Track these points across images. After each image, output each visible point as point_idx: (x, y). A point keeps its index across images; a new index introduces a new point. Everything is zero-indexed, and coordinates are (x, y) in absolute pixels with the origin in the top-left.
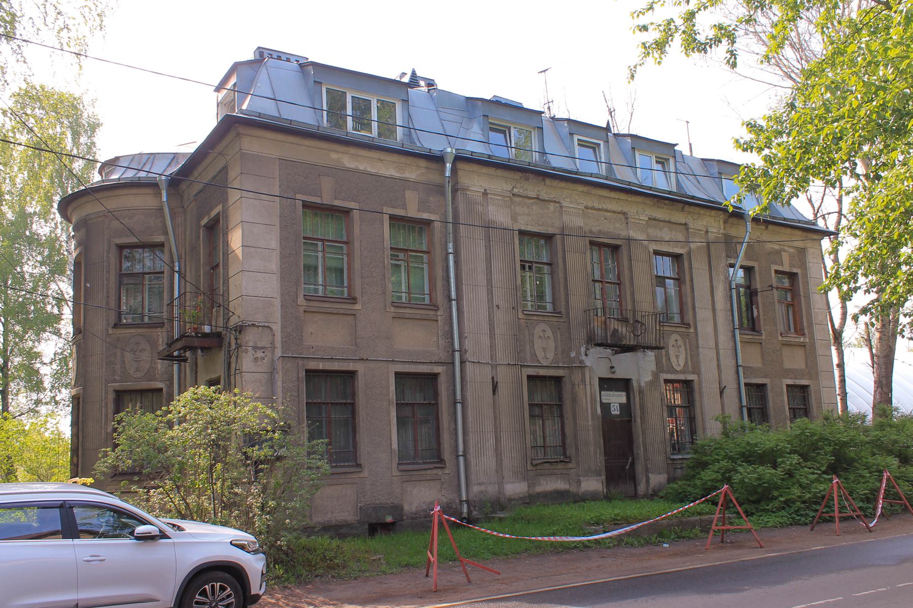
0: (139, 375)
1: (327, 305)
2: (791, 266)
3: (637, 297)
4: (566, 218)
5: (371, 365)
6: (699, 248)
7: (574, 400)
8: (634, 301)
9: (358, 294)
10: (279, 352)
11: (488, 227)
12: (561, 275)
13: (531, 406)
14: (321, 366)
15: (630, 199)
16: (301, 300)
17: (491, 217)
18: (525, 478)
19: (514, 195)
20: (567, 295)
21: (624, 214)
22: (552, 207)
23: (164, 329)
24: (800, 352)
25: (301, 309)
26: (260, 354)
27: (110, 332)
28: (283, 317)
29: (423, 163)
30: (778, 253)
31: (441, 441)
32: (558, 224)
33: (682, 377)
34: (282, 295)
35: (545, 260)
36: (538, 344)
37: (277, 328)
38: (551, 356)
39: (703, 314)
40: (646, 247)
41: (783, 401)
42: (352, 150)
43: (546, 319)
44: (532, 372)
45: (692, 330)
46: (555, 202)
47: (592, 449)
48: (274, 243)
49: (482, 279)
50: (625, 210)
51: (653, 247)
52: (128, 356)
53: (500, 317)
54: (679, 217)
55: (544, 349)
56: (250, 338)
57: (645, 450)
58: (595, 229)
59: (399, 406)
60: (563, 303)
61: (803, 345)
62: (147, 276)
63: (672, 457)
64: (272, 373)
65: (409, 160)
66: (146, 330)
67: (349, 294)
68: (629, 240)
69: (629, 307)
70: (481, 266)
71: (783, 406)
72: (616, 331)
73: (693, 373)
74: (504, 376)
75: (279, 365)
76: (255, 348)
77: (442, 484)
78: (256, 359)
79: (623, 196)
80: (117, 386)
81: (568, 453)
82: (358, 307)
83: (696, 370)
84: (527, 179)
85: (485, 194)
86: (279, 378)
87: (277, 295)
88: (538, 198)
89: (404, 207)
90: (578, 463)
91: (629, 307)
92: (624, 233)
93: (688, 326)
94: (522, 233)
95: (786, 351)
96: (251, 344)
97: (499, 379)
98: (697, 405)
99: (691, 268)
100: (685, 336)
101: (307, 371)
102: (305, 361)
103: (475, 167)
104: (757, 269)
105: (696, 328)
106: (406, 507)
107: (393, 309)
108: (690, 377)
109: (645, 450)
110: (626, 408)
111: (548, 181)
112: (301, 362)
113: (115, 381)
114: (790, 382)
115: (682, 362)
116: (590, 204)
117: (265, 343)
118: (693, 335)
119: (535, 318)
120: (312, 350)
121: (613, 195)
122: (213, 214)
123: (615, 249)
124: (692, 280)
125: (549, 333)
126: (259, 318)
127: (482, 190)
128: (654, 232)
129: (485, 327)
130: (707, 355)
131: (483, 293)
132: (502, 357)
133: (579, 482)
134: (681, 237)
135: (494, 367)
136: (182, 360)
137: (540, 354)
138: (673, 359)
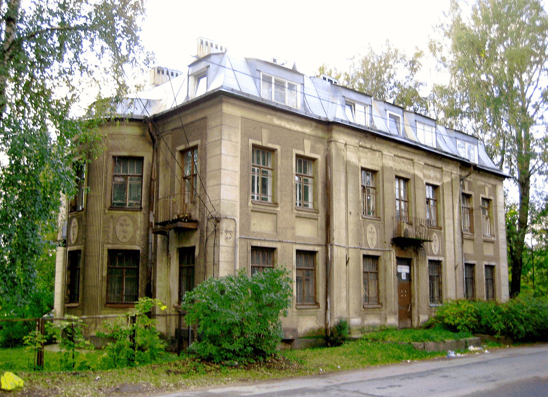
0: (125, 240)
1: (263, 207)
2: (489, 195)
3: (418, 210)
4: (384, 161)
5: (284, 245)
6: (448, 183)
7: (386, 270)
8: (416, 213)
9: (279, 202)
10: (238, 235)
11: (347, 164)
12: (381, 195)
13: (364, 272)
14: (259, 244)
15: (416, 152)
16: (250, 204)
17: (348, 159)
18: (360, 316)
19: (360, 146)
20: (384, 207)
21: (412, 160)
22: (377, 154)
23: (142, 212)
24: (491, 246)
25: (250, 209)
26: (229, 235)
27: (107, 211)
28: (241, 213)
29: (314, 124)
30: (483, 187)
31: (317, 291)
32: (380, 164)
33: (436, 258)
34: (240, 199)
35: (371, 185)
36: (369, 236)
37: (238, 220)
38: (375, 243)
39: (448, 222)
40: (422, 181)
41: (482, 274)
42: (279, 114)
43: (373, 221)
44: (365, 253)
45: (443, 231)
46: (379, 151)
47: (393, 299)
48: (238, 168)
49: (343, 195)
50: (413, 158)
51: (425, 181)
52: (118, 228)
53: (351, 219)
54: (439, 164)
55: (372, 239)
56: (224, 225)
57: (418, 301)
58: (398, 169)
59: (297, 269)
60: (382, 212)
61: (493, 242)
62: (129, 177)
63: (431, 305)
64: (235, 247)
65: (307, 122)
66: (130, 212)
67: (273, 200)
68: (414, 175)
69: (413, 216)
70: (343, 188)
71: (483, 277)
72: (406, 230)
73: (442, 256)
74: (352, 254)
75: (238, 243)
76: (227, 232)
77: (317, 318)
78: (227, 238)
79: (413, 150)
80: (110, 247)
81: (381, 301)
82: (278, 209)
83: (444, 255)
84: (366, 137)
85: (346, 144)
86: (238, 250)
87: (238, 200)
88: (371, 149)
89: (303, 149)
90: (386, 309)
91: (413, 216)
92: (412, 172)
93: (440, 229)
94: (363, 169)
95: (485, 245)
96: (224, 229)
97: (350, 255)
98: (443, 275)
99: (443, 194)
100: (439, 234)
101: (252, 247)
102: (251, 241)
103: (342, 129)
104: (473, 196)
105: (445, 230)
106: (299, 331)
107: (296, 212)
108: (441, 259)
109: (418, 301)
110: (409, 275)
111: (377, 139)
112: (249, 241)
113: (109, 243)
114: (486, 263)
115: (437, 250)
116: (396, 153)
117: (231, 228)
118: (443, 234)
119: (368, 220)
120: (254, 234)
121: (408, 149)
122: (191, 144)
123: (406, 180)
124: (443, 201)
125: (374, 230)
126: (228, 213)
127: (344, 142)
128: (426, 172)
129: (344, 225)
130: (449, 246)
131: (343, 205)
132: (352, 244)
133: (386, 319)
134: (438, 176)
135: (347, 249)
136: (163, 233)
137: (369, 242)
138: (433, 248)
